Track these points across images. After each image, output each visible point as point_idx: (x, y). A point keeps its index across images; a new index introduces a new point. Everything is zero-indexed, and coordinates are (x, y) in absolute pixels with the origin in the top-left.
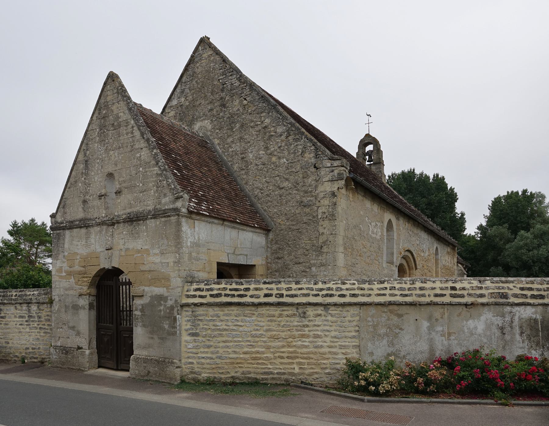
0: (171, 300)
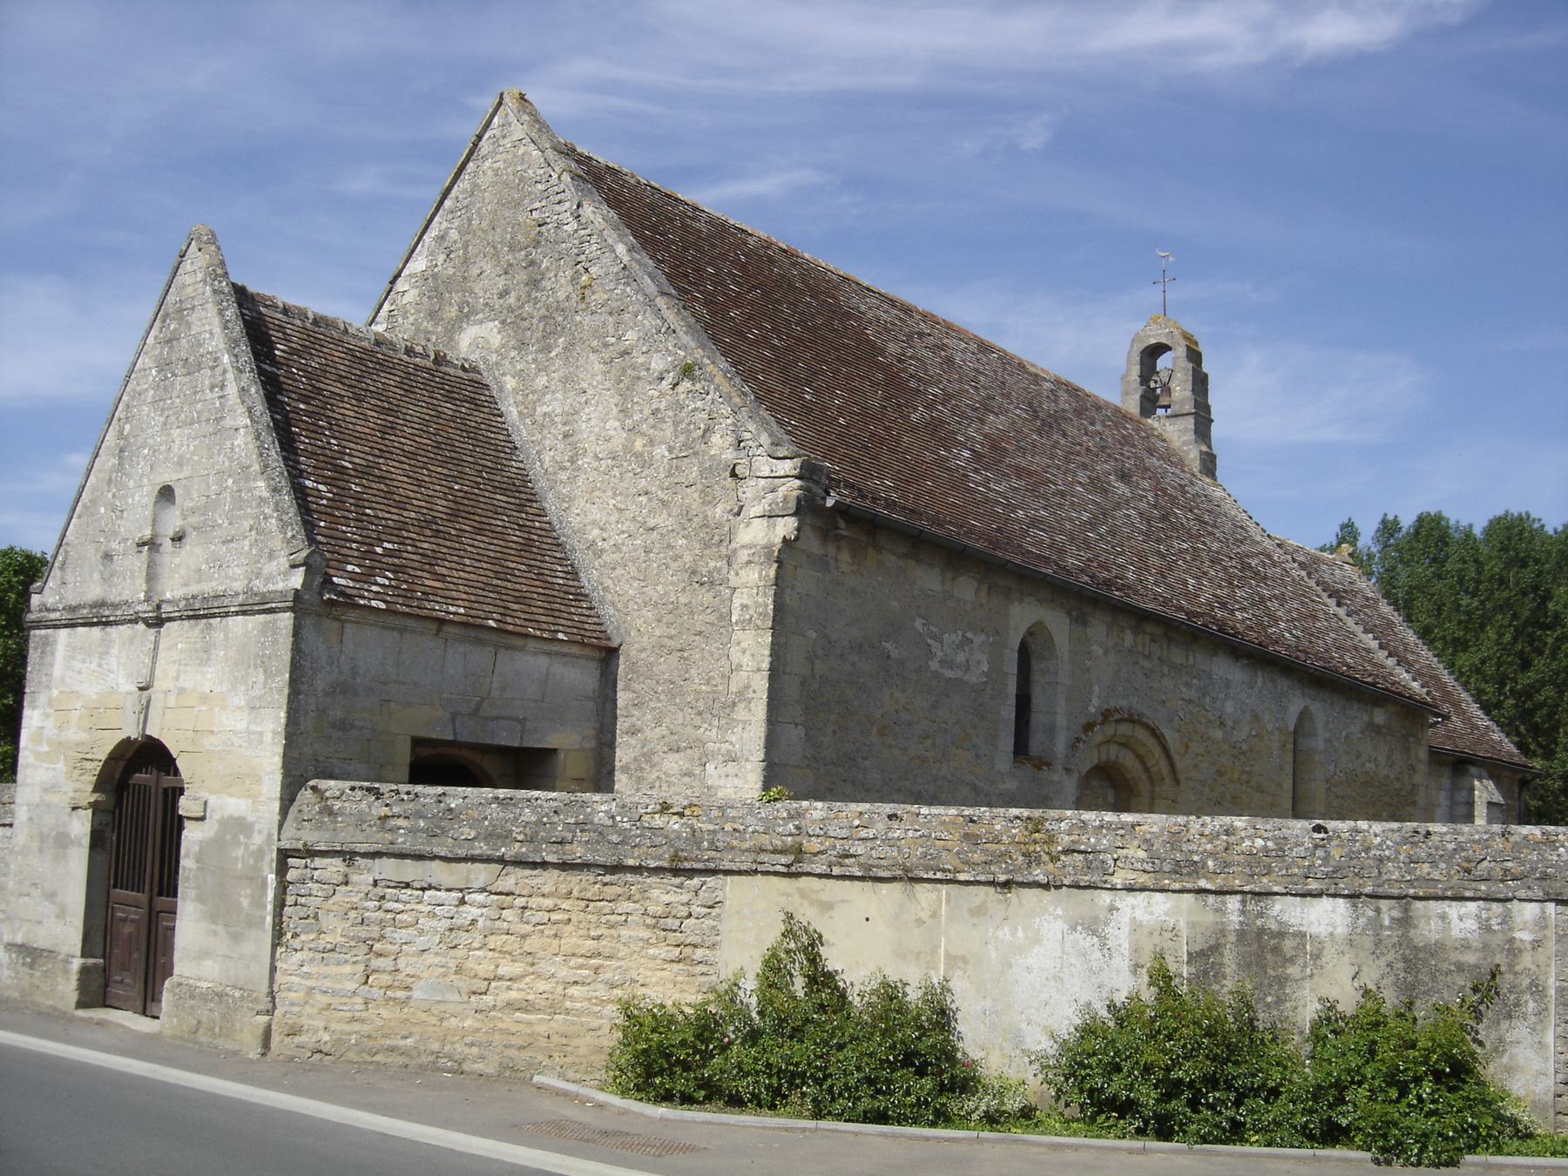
0: (260, 832)
